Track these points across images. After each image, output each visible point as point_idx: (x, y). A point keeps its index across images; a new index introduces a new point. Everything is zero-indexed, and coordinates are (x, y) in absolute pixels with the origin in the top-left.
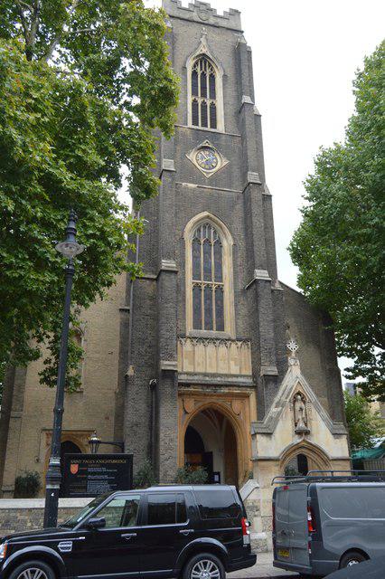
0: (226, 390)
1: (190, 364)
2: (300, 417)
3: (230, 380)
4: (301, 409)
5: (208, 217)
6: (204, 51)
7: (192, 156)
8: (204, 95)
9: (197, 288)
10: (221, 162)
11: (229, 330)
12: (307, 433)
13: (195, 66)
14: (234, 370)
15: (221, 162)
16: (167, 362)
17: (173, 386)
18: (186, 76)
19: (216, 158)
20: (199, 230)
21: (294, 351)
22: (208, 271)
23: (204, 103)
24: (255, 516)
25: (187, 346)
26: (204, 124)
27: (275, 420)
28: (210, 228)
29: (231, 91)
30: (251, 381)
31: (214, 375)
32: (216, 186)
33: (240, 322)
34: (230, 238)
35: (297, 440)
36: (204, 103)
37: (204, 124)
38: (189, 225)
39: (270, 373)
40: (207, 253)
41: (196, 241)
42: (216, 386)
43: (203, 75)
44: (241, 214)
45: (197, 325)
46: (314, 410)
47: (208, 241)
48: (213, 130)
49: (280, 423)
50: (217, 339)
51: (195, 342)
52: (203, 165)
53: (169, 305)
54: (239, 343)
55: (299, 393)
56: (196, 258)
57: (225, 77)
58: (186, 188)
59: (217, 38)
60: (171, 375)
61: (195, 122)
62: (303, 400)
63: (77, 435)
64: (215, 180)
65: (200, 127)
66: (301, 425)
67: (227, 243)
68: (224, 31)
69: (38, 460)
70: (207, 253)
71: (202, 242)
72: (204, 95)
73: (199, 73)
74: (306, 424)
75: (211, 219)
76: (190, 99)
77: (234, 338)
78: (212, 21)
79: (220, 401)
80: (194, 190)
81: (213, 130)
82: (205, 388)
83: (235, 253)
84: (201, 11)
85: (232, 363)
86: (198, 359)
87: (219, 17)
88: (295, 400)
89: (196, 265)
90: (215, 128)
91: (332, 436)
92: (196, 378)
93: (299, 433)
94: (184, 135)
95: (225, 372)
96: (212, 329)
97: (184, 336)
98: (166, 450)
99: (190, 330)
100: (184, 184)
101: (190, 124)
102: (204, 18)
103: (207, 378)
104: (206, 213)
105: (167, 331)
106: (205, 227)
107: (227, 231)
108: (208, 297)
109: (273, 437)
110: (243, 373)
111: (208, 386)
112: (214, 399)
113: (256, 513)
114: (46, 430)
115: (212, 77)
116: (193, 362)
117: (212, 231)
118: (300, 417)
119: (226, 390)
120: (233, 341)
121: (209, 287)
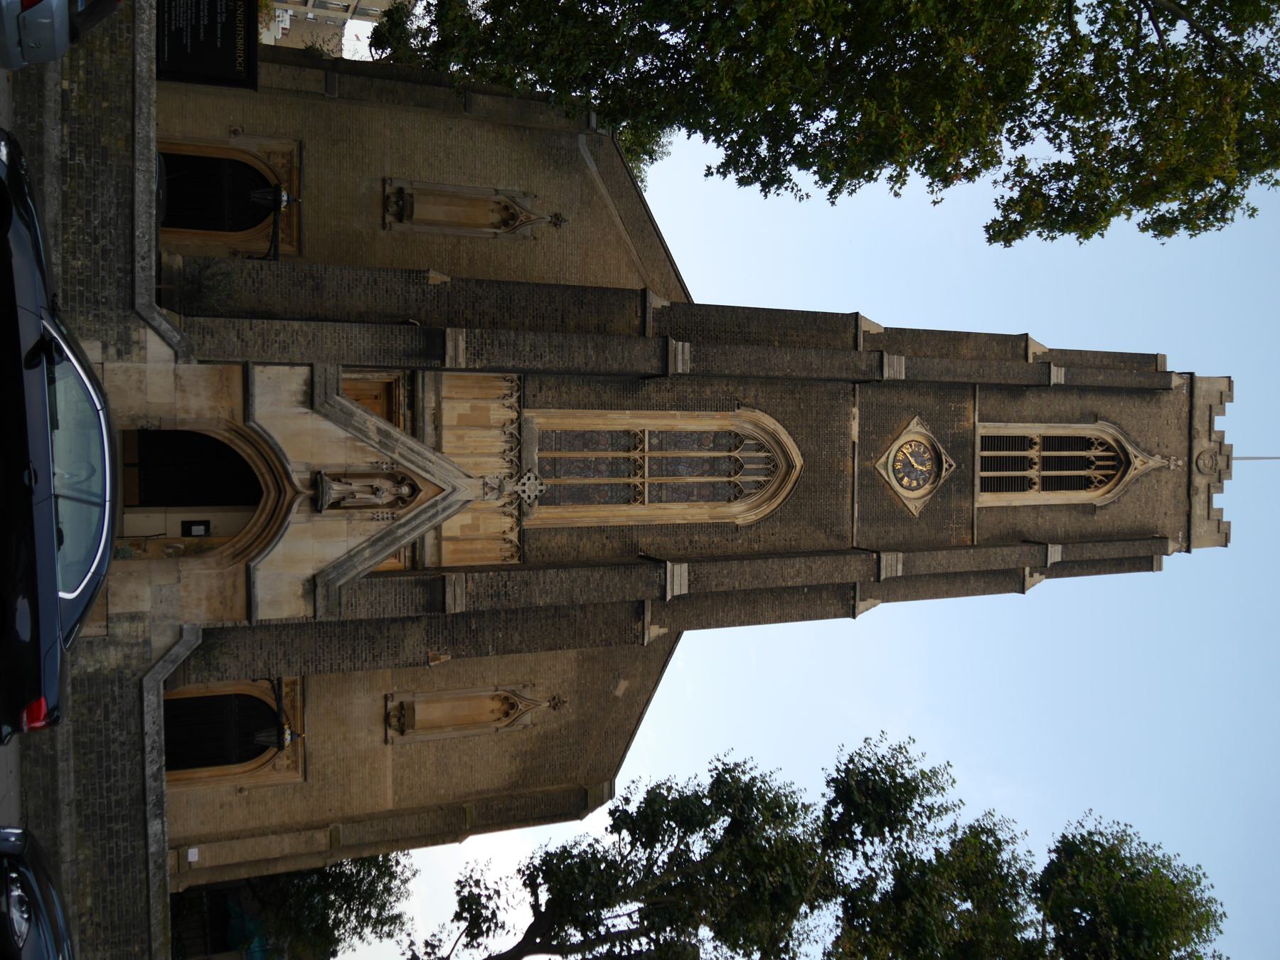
1: (461, 417)
4: (375, 491)
5: (790, 466)
6: (1137, 463)
7: (915, 434)
8: (1047, 463)
9: (632, 439)
10: (914, 497)
12: (316, 505)
13: (1101, 444)
15: (914, 497)
16: (462, 345)
17: (408, 355)
18: (1079, 421)
19: (919, 487)
20: (760, 447)
22: (669, 467)
23: (1029, 463)
25: (500, 413)
26: (987, 464)
27: (344, 420)
28: (769, 473)
29: (1065, 523)
32: (860, 485)
33: (562, 539)
34: (752, 517)
35: (299, 476)
36: (1029, 463)
37: (987, 464)
38: (770, 422)
39: (449, 597)
40: (713, 466)
41: (736, 440)
43: (1086, 463)
45: (547, 439)
46: (374, 528)
47: (738, 467)
48: (977, 482)
49: (341, 433)
51: (512, 429)
52: (900, 456)
53: (591, 352)
54: (513, 536)
55: (415, 490)
56: (698, 439)
57: (1090, 509)
58: (848, 416)
59: (1166, 493)
60: (432, 351)
61: (989, 442)
62: (400, 501)
64: (872, 483)
65: (979, 454)
66: (335, 490)
67: (740, 512)
68: (1183, 508)
70: (713, 466)
71: (735, 454)
72: (1047, 463)
76: (1035, 430)
77: (526, 523)
78: (1200, 481)
80: (847, 435)
81: (977, 482)
84: (1213, 457)
88: (398, 478)
90: (984, 489)
91: (309, 572)
94: (959, 414)
97: (522, 404)
99: (539, 420)
100: (856, 411)
101: (984, 429)
102: (1201, 463)
104: (798, 461)
105: (534, 347)
106: (769, 460)
107: (766, 510)
110: (444, 544)
113: (112, 351)
115: (1085, 484)
117: (761, 479)
120: (519, 521)
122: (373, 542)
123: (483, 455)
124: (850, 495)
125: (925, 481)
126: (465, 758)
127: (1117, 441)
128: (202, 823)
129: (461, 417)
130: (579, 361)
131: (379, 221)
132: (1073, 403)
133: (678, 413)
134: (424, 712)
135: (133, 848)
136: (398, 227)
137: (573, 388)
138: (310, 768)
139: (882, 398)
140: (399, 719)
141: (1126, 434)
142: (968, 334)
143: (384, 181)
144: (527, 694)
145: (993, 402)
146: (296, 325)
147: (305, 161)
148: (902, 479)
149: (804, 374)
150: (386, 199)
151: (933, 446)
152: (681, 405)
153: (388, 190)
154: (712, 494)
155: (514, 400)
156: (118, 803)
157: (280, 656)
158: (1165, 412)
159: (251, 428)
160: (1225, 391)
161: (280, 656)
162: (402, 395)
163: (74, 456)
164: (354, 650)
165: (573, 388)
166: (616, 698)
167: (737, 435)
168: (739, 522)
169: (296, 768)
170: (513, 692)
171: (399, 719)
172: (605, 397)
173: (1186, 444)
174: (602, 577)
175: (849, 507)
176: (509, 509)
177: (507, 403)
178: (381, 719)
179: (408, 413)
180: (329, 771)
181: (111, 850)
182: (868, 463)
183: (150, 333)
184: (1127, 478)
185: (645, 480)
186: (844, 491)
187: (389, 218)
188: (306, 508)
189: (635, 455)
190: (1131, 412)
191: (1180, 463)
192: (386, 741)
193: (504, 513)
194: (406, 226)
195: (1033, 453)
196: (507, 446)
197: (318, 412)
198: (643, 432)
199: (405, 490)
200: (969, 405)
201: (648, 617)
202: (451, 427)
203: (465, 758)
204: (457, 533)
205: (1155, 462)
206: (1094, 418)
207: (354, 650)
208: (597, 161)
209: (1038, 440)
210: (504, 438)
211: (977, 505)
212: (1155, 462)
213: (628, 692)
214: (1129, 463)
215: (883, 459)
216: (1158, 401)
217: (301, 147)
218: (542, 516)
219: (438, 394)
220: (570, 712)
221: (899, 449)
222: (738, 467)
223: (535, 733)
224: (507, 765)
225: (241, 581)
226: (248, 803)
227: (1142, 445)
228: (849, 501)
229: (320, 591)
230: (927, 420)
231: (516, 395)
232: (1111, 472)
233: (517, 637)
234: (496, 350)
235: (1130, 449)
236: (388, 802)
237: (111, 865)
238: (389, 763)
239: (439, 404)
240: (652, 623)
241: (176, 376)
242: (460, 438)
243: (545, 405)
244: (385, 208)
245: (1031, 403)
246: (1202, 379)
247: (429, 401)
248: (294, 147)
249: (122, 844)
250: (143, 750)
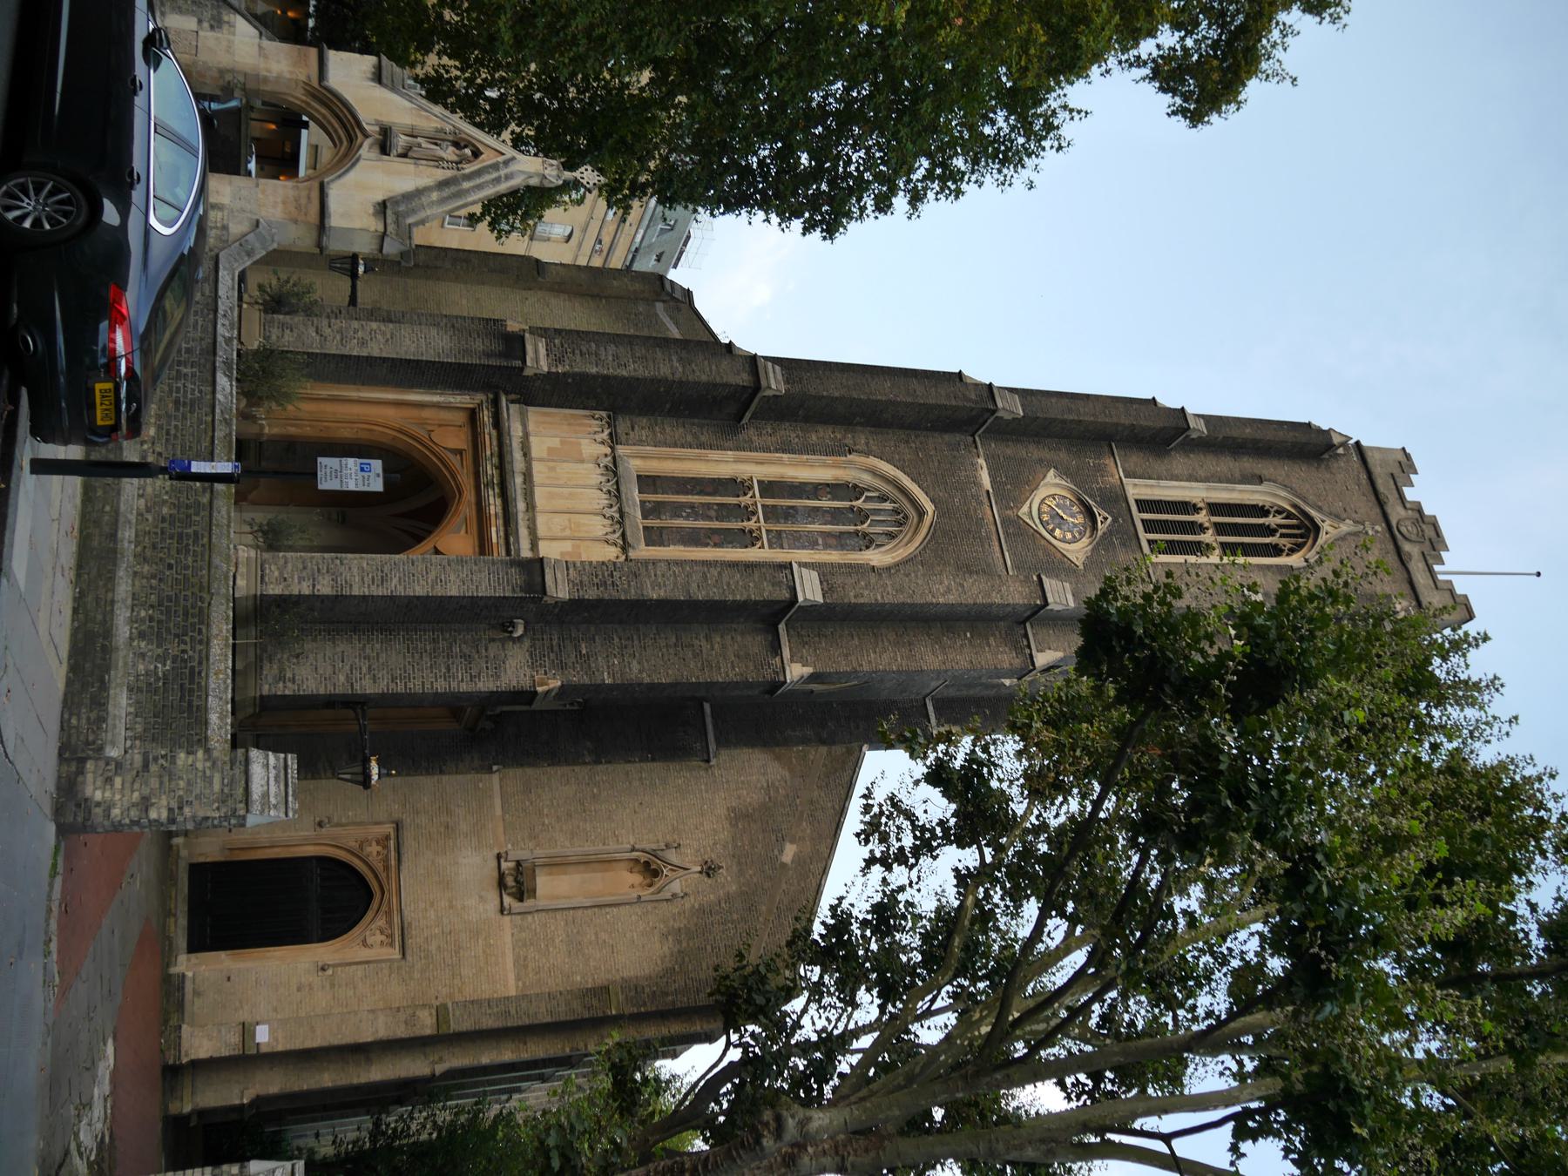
0: (494, 505)
1: (550, 450)
5: (921, 514)
8: (1221, 529)
9: (736, 486)
16: (542, 351)
19: (1075, 540)
20: (883, 499)
21: (577, 174)
23: (1202, 529)
24: (200, 22)
32: (1007, 534)
37: (1149, 526)
40: (835, 516)
41: (855, 491)
43: (1270, 531)
45: (648, 482)
46: (441, 174)
49: (407, 104)
50: (621, 511)
55: (476, 154)
56: (815, 490)
61: (1144, 505)
64: (1018, 531)
66: (401, 141)
67: (876, 557)
70: (835, 516)
71: (859, 503)
73: (1272, 520)
79: (465, 508)
80: (979, 485)
82: (495, 460)
86: (566, 469)
91: (380, 198)
94: (1101, 469)
96: (645, 517)
97: (614, 440)
98: (340, 331)
99: (639, 460)
100: (981, 461)
101: (1137, 490)
102: (1403, 529)
103: (519, 480)
104: (929, 507)
105: (616, 357)
106: (896, 512)
107: (902, 553)
112: (469, 495)
113: (206, 25)
115: (1276, 551)
116: (554, 456)
119: (494, 505)
121: (748, 513)
122: (442, 185)
123: (577, 486)
125: (1082, 534)
126: (603, 936)
127: (1295, 506)
128: (275, 1010)
129: (550, 450)
132: (1226, 464)
133: (785, 456)
134: (547, 886)
135: (200, 392)
137: (668, 430)
138: (409, 942)
139: (1009, 451)
140: (516, 884)
141: (1304, 500)
142: (1088, 396)
144: (672, 856)
145: (1136, 459)
146: (374, 325)
148: (1053, 530)
149: (909, 400)
152: (785, 448)
154: (840, 541)
155: (605, 435)
156: (188, 351)
157: (364, 670)
158: (1339, 477)
159: (326, 89)
160: (1404, 465)
161: (364, 670)
162: (486, 416)
163: (164, 100)
164: (448, 669)
165: (668, 430)
166: (784, 865)
167: (855, 486)
169: (391, 945)
170: (653, 853)
171: (516, 884)
172: (703, 438)
173: (1378, 510)
174: (720, 574)
175: (999, 554)
177: (599, 437)
178: (495, 884)
179: (494, 433)
180: (433, 948)
181: (178, 389)
183: (239, 18)
184: (1320, 541)
185: (758, 523)
186: (989, 538)
188: (376, 150)
190: (1301, 474)
191: (1378, 528)
192: (502, 912)
193: (607, 542)
195: (1202, 517)
196: (604, 479)
197: (385, 86)
199: (468, 151)
200: (1109, 461)
201: (786, 653)
202: (541, 460)
203: (603, 936)
204: (545, 455)
205: (1346, 527)
206: (1260, 480)
207: (448, 669)
208: (676, 324)
209: (1201, 505)
210: (599, 471)
212: (1346, 527)
213: (797, 859)
214: (1317, 529)
215: (1025, 508)
216: (1328, 468)
219: (525, 426)
220: (727, 880)
221: (1042, 502)
222: (862, 516)
223: (687, 906)
224: (658, 945)
225: (315, 195)
226: (332, 985)
227: (1325, 508)
228: (997, 549)
229: (389, 212)
230: (1064, 472)
231: (607, 432)
233: (635, 666)
234: (578, 358)
235: (1313, 513)
236: (510, 986)
237: (177, 402)
238: (508, 939)
239: (526, 435)
240: (792, 661)
241: (260, 47)
242: (552, 469)
243: (640, 442)
245: (1179, 462)
246: (1372, 448)
247: (516, 430)
249: (190, 386)
250: (216, 311)
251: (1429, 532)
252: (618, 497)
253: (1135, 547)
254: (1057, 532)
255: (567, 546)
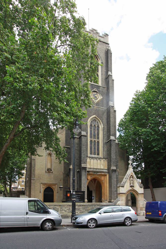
1: (89, 165)
2: (132, 182)
3: (101, 170)
4: (132, 180)
5: (95, 117)
11: (101, 155)
12: (133, 186)
14: (102, 167)
19: (98, 96)
20: (92, 122)
22: (95, 136)
28: (95, 121)
30: (107, 171)
31: (97, 169)
32: (98, 106)
33: (104, 153)
34: (102, 125)
35: (131, 188)
38: (89, 120)
41: (91, 125)
42: (97, 172)
44: (106, 117)
45: (91, 154)
47: (95, 126)
60: (85, 168)
63: (52, 185)
66: (132, 184)
67: (101, 127)
68: (102, 43)
69: (40, 192)
70: (94, 130)
71: (93, 126)
74: (133, 184)
75: (96, 118)
83: (103, 130)
84: (94, 33)
85: (102, 165)
87: (101, 37)
88: (130, 178)
89: (91, 134)
92: (91, 169)
93: (131, 186)
95: (100, 168)
97: (87, 157)
103: (94, 170)
104: (94, 116)
106: (94, 121)
107: (101, 122)
108: (95, 144)
109: (124, 187)
110: (104, 169)
111: (95, 172)
112: (96, 176)
114: (42, 183)
116: (90, 165)
117: (96, 122)
118: (132, 182)
120: (102, 159)
121: (95, 141)
124: (99, 108)
129: (89, 165)
130: (85, 149)
131: (51, 173)
136: (53, 171)
143: (46, 172)
147: (44, 183)
150: (49, 172)
151: (92, 92)
153: (47, 171)
168: (103, 127)
176: (101, 160)
182: (95, 104)
186: (99, 109)
187: (51, 172)
189: (96, 141)
194: (52, 169)
198: (90, 139)
211: (101, 86)
217: (42, 183)
218: (101, 155)
222: (95, 126)
232: (96, 57)
242: (92, 165)
244: (50, 172)
248: (42, 184)
251: (95, 32)
252: (96, 158)
253: (99, 87)
254: (97, 98)
255: (102, 165)
